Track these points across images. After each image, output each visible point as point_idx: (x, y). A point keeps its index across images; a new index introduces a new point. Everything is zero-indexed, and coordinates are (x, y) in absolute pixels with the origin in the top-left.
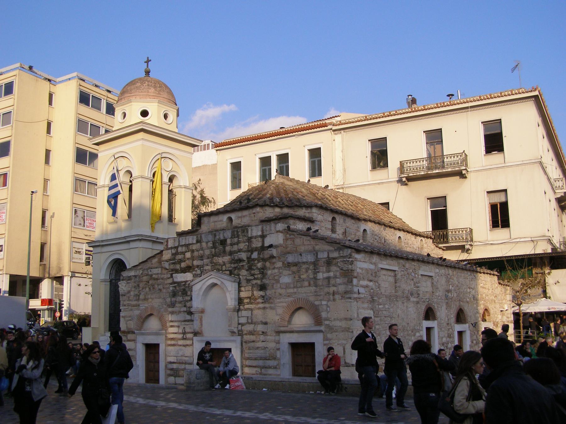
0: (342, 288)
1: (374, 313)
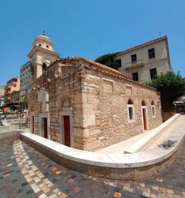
0: (78, 87)
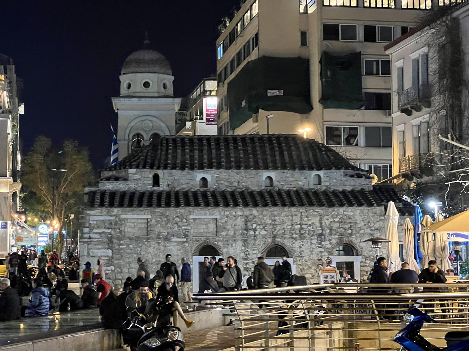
1: (112, 251)
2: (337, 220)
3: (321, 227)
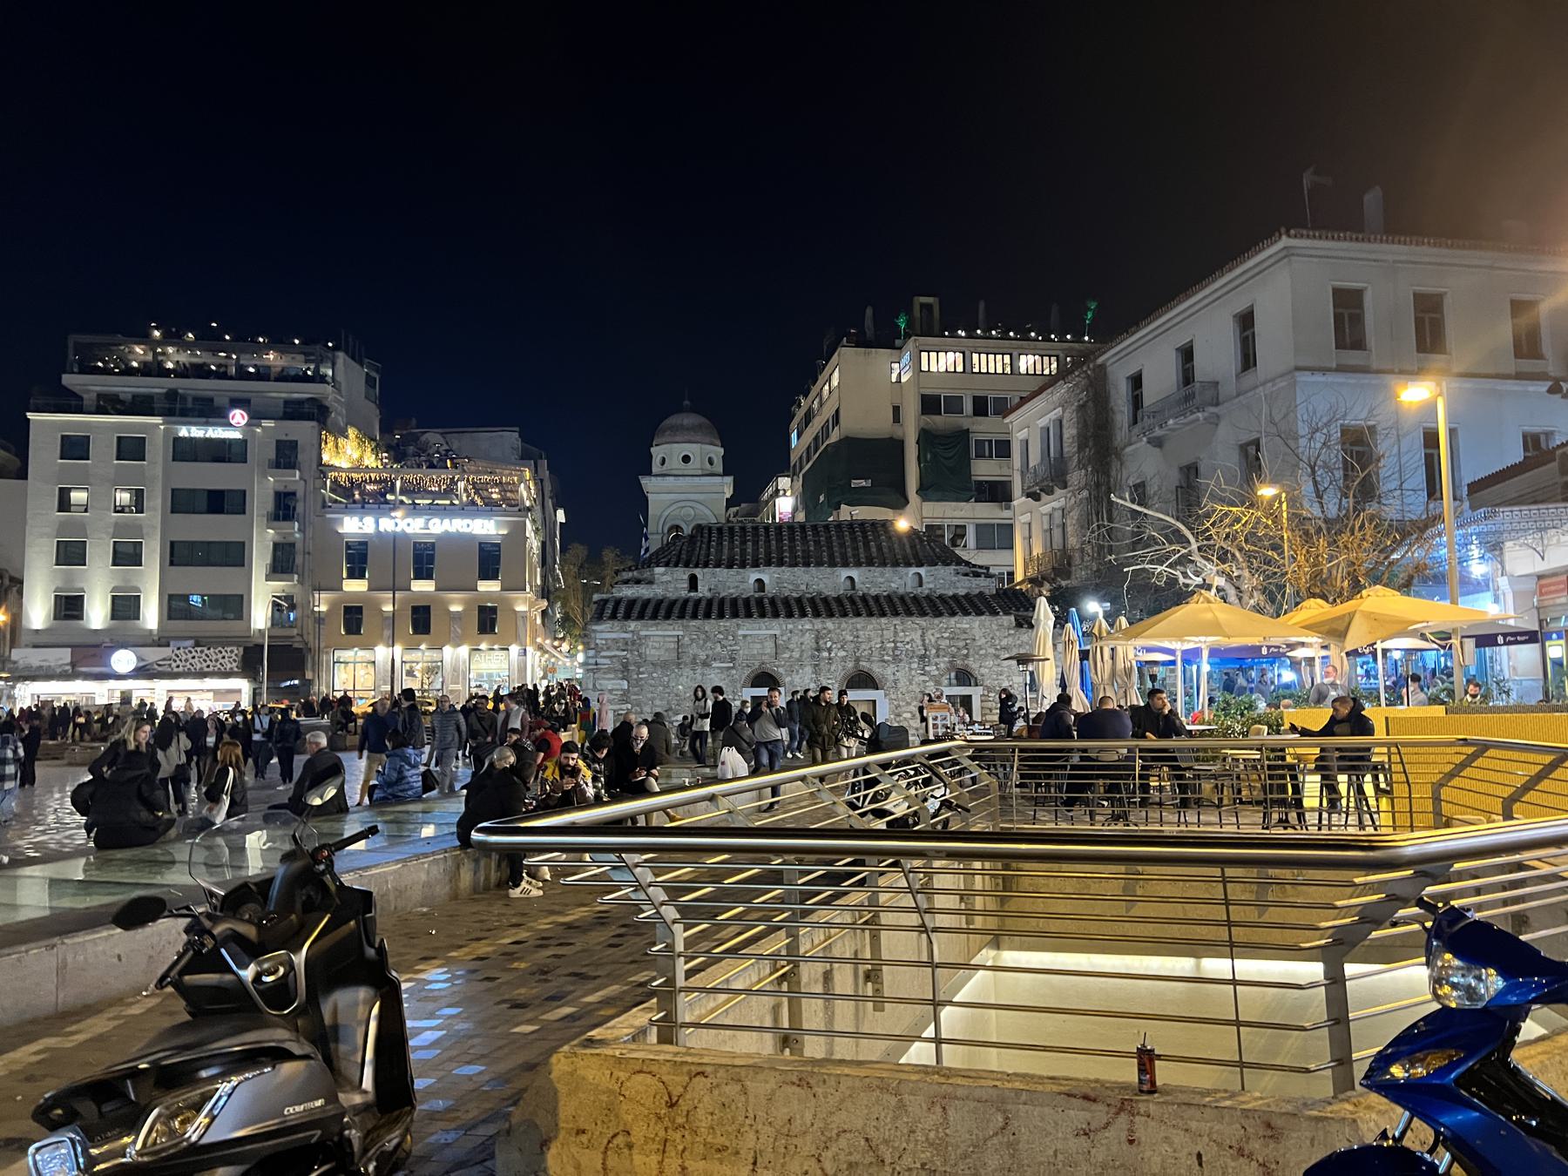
2: (946, 635)
3: (924, 645)
